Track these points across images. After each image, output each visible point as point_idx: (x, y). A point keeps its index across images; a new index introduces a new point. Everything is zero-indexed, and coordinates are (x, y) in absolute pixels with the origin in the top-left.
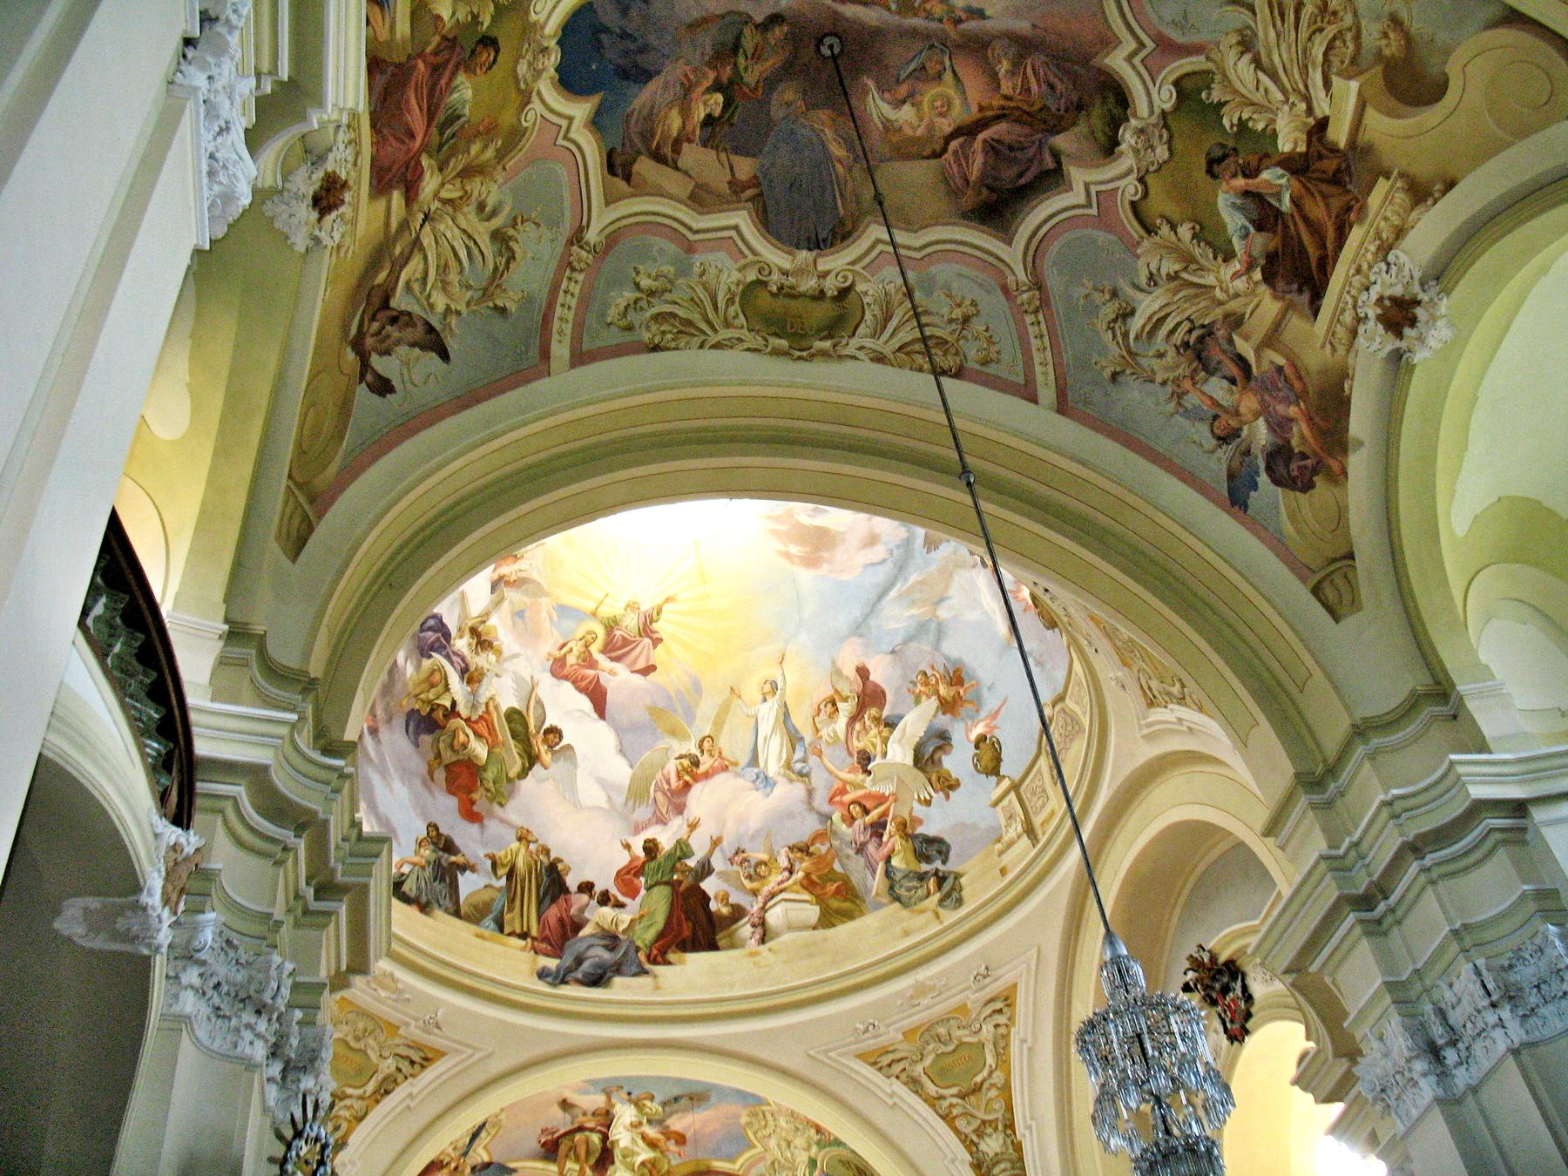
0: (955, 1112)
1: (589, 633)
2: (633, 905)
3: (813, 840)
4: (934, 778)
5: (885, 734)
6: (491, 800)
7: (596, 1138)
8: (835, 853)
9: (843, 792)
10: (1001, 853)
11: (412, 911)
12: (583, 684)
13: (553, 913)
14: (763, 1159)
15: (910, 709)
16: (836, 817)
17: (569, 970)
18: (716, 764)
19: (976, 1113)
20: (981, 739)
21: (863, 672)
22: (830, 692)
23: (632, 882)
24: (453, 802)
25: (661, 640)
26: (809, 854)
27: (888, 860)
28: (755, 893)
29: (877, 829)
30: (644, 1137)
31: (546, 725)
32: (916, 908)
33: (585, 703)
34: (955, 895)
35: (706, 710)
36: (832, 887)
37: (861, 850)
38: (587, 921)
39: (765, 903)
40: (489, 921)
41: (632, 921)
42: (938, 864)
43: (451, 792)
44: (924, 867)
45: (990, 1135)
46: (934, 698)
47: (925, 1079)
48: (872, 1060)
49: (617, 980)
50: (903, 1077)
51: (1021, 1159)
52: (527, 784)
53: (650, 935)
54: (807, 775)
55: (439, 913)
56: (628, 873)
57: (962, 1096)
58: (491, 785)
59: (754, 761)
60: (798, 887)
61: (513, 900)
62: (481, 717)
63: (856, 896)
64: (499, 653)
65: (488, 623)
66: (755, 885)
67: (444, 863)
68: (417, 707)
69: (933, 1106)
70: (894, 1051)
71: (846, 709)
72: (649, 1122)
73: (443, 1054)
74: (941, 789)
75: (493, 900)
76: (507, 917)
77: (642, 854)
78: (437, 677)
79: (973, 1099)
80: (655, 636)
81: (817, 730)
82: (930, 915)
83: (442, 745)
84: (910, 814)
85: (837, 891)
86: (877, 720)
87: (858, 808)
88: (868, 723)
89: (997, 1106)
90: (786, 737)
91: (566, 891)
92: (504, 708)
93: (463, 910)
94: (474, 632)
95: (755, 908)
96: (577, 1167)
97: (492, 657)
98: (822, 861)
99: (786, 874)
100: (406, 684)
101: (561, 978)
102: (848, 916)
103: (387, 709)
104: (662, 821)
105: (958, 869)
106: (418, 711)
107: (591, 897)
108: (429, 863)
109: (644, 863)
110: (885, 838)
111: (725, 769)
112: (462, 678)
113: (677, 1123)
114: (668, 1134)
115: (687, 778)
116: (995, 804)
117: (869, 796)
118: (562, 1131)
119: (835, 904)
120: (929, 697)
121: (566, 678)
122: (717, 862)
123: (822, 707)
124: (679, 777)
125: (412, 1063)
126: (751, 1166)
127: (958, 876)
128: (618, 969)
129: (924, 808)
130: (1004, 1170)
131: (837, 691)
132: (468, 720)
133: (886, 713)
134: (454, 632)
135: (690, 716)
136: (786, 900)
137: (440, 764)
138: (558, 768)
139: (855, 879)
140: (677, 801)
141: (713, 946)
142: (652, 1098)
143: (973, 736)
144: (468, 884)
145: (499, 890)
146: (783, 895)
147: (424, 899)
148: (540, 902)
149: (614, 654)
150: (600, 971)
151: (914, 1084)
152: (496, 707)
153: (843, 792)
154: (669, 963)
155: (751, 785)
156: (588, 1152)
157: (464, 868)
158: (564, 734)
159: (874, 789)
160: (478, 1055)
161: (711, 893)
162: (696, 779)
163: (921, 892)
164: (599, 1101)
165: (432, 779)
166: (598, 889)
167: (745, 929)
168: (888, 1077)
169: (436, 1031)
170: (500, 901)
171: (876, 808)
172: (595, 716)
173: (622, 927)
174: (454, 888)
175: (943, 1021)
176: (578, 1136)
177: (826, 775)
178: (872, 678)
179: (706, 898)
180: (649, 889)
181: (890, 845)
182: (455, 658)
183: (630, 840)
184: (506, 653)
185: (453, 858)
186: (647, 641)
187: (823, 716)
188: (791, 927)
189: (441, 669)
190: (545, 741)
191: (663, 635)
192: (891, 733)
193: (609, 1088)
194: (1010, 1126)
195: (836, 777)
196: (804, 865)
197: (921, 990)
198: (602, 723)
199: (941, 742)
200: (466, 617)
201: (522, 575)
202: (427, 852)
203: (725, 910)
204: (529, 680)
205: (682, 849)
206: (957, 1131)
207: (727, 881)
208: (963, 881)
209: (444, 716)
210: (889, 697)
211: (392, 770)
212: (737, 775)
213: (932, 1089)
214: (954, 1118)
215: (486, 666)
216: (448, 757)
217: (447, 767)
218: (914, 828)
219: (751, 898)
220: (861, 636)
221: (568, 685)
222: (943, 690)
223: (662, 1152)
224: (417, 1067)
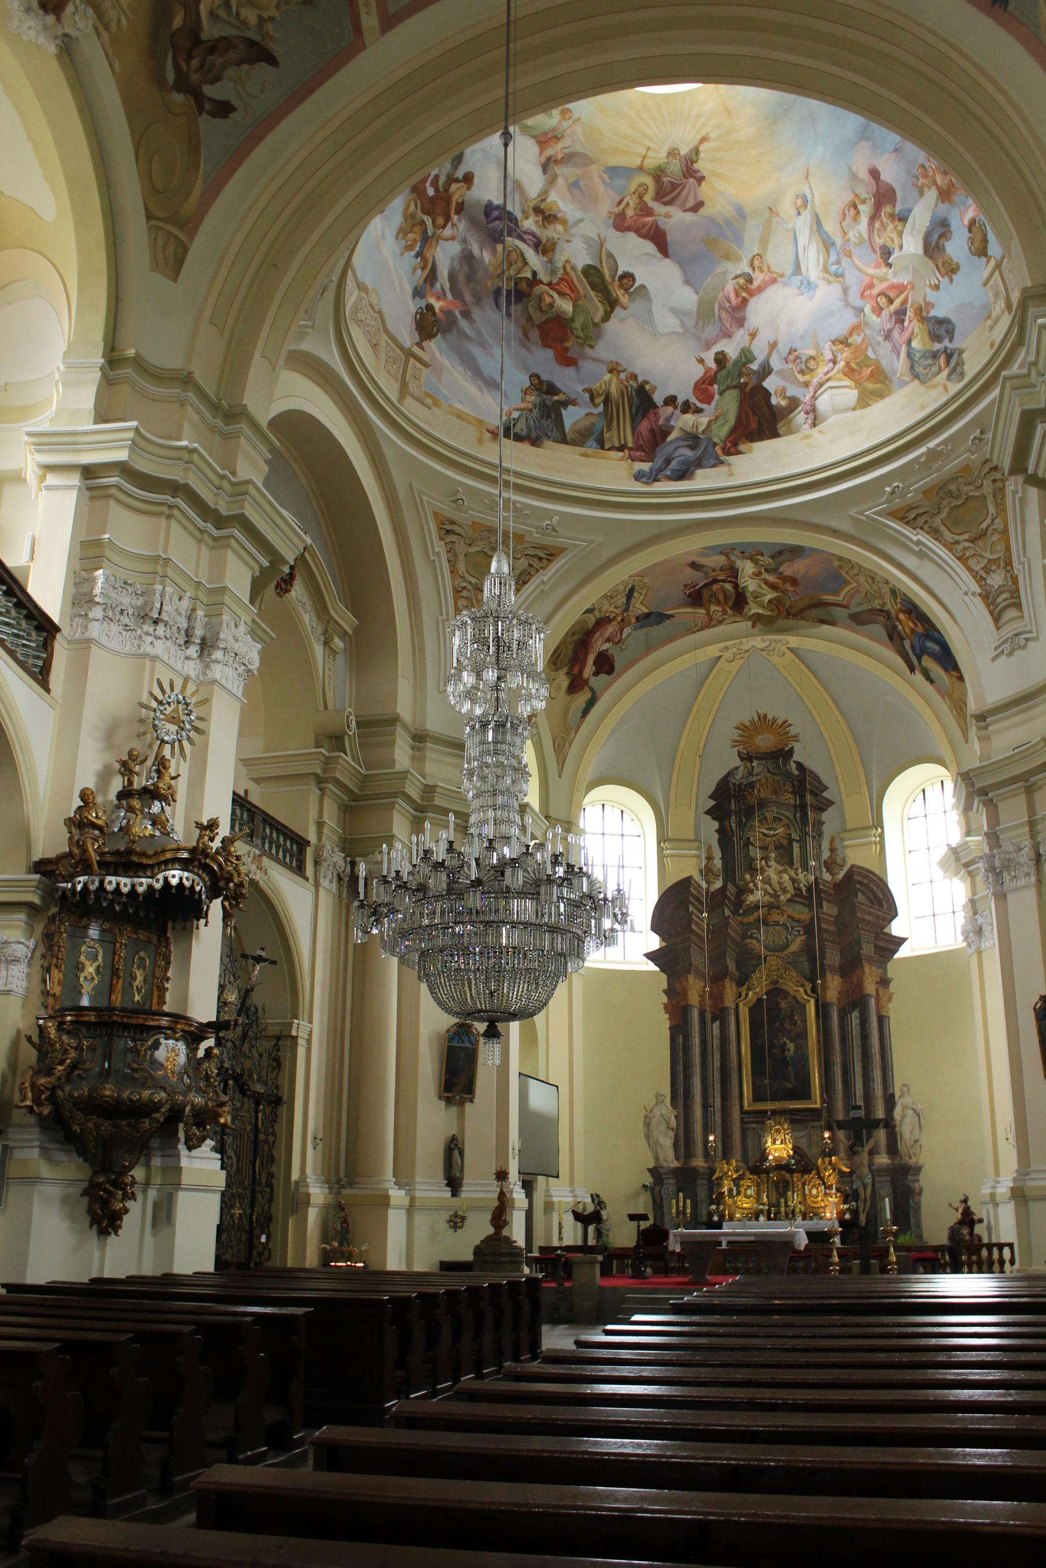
0: (968, 554)
1: (640, 185)
2: (709, 409)
3: (851, 333)
4: (940, 264)
5: (899, 228)
6: (582, 345)
7: (729, 587)
8: (867, 343)
9: (871, 286)
10: (991, 328)
11: (526, 447)
12: (645, 231)
13: (644, 426)
14: (858, 591)
15: (917, 201)
16: (868, 309)
17: (660, 470)
18: (767, 278)
19: (983, 553)
20: (973, 222)
21: (875, 174)
22: (851, 197)
23: (707, 389)
24: (550, 353)
25: (702, 179)
26: (848, 345)
27: (909, 342)
28: (806, 385)
29: (900, 316)
30: (766, 582)
31: (620, 272)
32: (930, 383)
33: (649, 247)
34: (959, 369)
35: (752, 232)
36: (867, 372)
37: (888, 336)
38: (673, 428)
39: (815, 393)
40: (591, 442)
41: (710, 422)
42: (946, 343)
43: (546, 345)
44: (937, 346)
45: (994, 571)
46: (933, 188)
47: (943, 528)
48: (901, 516)
49: (699, 472)
50: (926, 527)
51: (1018, 590)
52: (611, 325)
53: (724, 431)
54: (842, 276)
55: (548, 443)
56: (703, 383)
57: (973, 540)
58: (581, 334)
59: (797, 269)
60: (840, 375)
61: (609, 422)
62: (561, 279)
63: (886, 378)
64: (564, 222)
65: (549, 200)
66: (806, 378)
67: (548, 402)
69: (950, 550)
70: (917, 507)
71: (865, 210)
72: (767, 571)
73: (562, 550)
74: (947, 274)
75: (593, 424)
76: (607, 435)
77: (713, 365)
78: (514, 256)
79: (980, 543)
80: (698, 175)
81: (845, 234)
82: (940, 388)
83: (531, 310)
84: (924, 299)
85: (872, 375)
86: (892, 216)
87: (884, 299)
88: (885, 220)
89: (999, 547)
90: (821, 247)
91: (653, 405)
92: (580, 268)
93: (568, 438)
94: (537, 210)
95: (808, 398)
96: (720, 609)
97: (560, 228)
98: (859, 351)
99: (831, 365)
100: (486, 270)
101: (653, 477)
102: (880, 395)
103: (474, 293)
104: (728, 335)
105: (961, 346)
107: (675, 407)
108: (535, 406)
109: (716, 373)
110: (906, 324)
111: (774, 281)
112: (536, 250)
113: (787, 569)
114: (784, 579)
115: (744, 294)
116: (986, 284)
117: (893, 287)
118: (701, 585)
119: (870, 386)
120: (930, 188)
121: (628, 229)
122: (775, 363)
123: (846, 211)
124: (737, 295)
125: (541, 559)
126: (852, 597)
127: (961, 352)
128: (699, 464)
129: (934, 293)
130: (1005, 600)
131: (856, 195)
132: (549, 285)
133: (897, 209)
134: (518, 214)
135: (739, 238)
136: (831, 388)
137: (532, 325)
138: (636, 307)
139: (885, 364)
140: (739, 315)
141: (775, 434)
142: (762, 555)
143: (966, 223)
144: (571, 417)
145: (598, 415)
146: (829, 384)
147: (534, 435)
148: (633, 420)
149: (667, 199)
150: (685, 467)
151: (935, 533)
152: (573, 268)
153: (871, 286)
154: (740, 453)
155: (797, 291)
156: (726, 598)
157: (565, 404)
158: (637, 276)
159: (895, 281)
160: (592, 546)
161: (772, 390)
162: (751, 294)
163: (934, 369)
164: (722, 560)
165: (528, 339)
166: (680, 401)
167: (800, 417)
168: (914, 529)
169: (554, 533)
170: (601, 423)
171: (898, 296)
172: (660, 256)
173: (701, 429)
174: (559, 421)
175: (953, 479)
176: (715, 587)
177: (856, 273)
178: (882, 178)
179: (767, 394)
180: (721, 394)
181: (910, 329)
182: (526, 237)
183: (703, 356)
184: (571, 221)
185: (556, 398)
186: (692, 180)
187: (848, 220)
188: (836, 411)
189: (516, 248)
190: (621, 286)
191: (705, 174)
192: (904, 226)
193: (726, 550)
194: (1009, 563)
195: (865, 273)
196: (844, 355)
197: (932, 454)
198: (667, 261)
199: (943, 230)
200: (527, 200)
201: (569, 150)
202: (532, 398)
203: (783, 403)
204: (597, 238)
205: (747, 356)
206: (970, 569)
207: (783, 378)
208: (965, 356)
209: (528, 285)
210: (899, 193)
211: (490, 341)
212: (785, 285)
213: (949, 536)
214: (967, 558)
215: (556, 236)
216: (538, 317)
217: (539, 327)
218: (928, 313)
219: (804, 390)
220: (867, 139)
221: (632, 236)
222: (939, 179)
223: (783, 592)
224: (545, 561)
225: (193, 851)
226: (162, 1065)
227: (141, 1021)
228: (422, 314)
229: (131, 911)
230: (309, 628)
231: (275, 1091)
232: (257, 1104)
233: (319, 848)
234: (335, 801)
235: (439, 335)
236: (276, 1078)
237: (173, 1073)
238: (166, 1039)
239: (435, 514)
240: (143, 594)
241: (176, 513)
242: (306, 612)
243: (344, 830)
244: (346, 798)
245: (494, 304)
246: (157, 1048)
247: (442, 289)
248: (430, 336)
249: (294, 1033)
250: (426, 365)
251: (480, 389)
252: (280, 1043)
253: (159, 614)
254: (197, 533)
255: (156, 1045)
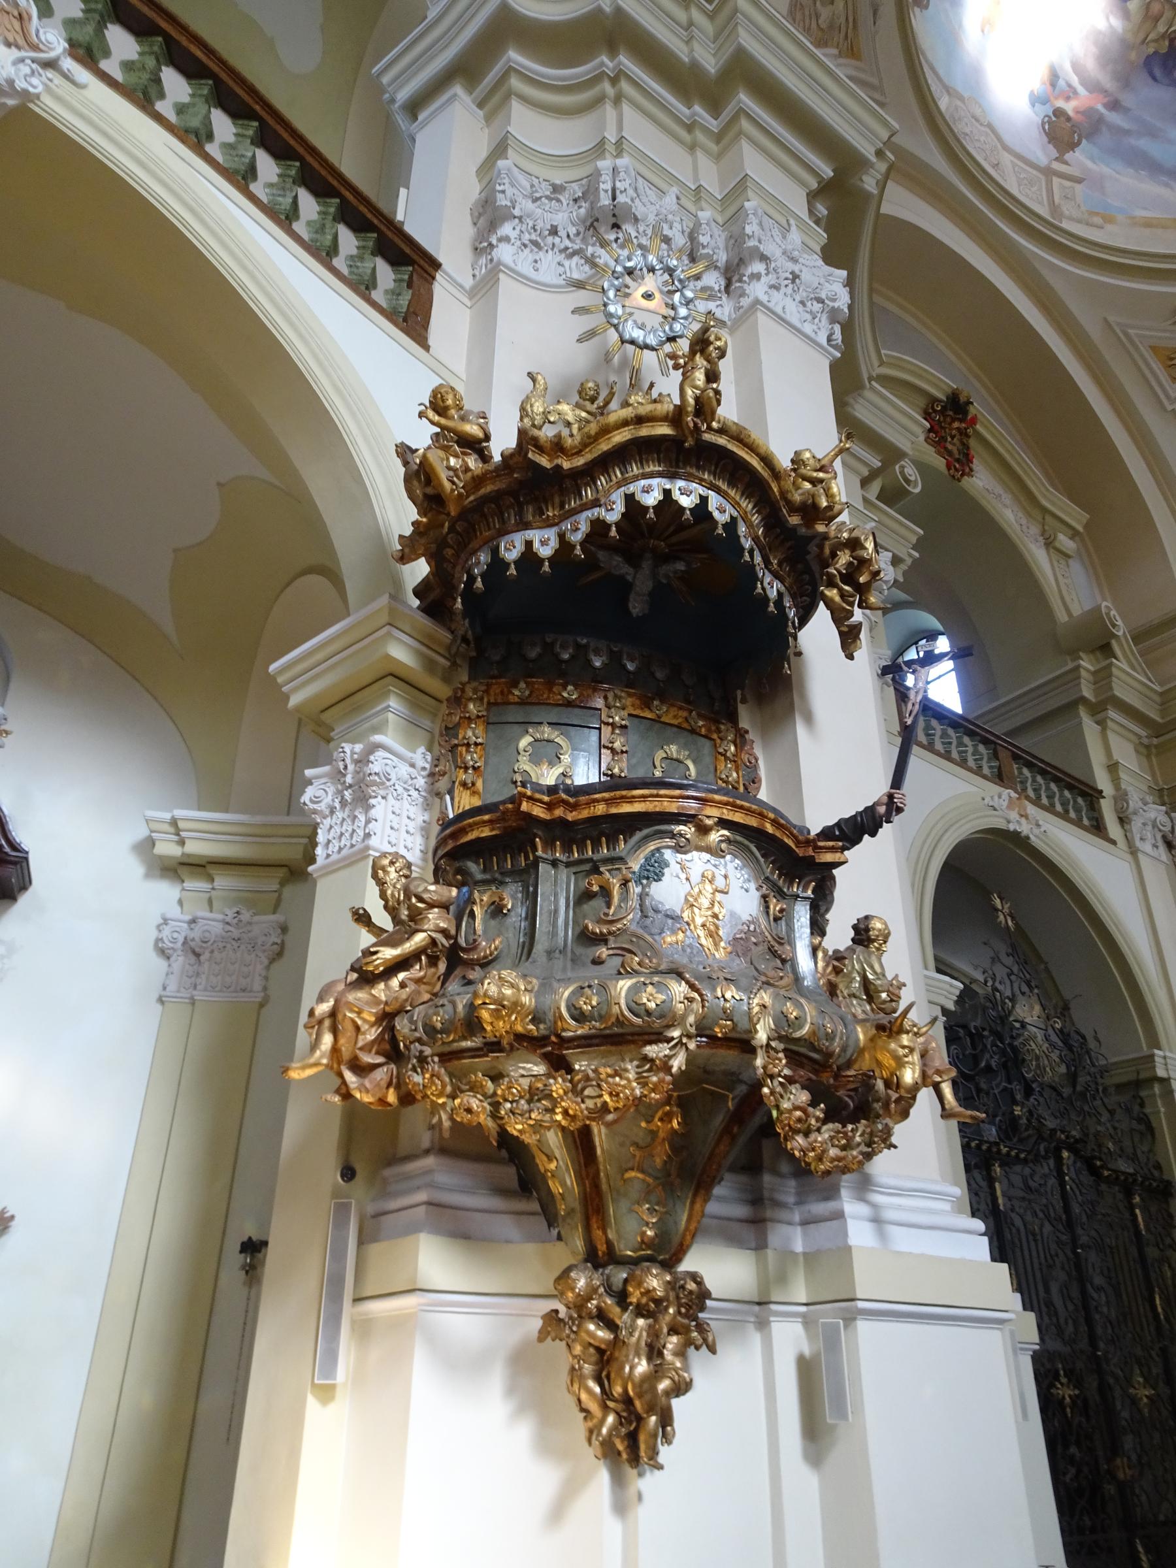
68: (1151, 50)
106: (1156, 53)
225: (676, 417)
226: (675, 918)
227: (600, 809)
228: (1049, 122)
229: (630, 667)
230: (1018, 528)
231: (1156, 1173)
232: (1129, 1194)
233: (1121, 798)
234: (1129, 740)
235: (1084, 141)
236: (1150, 1151)
237: (713, 935)
238: (679, 849)
239: (1154, 349)
240: (585, 196)
241: (625, 86)
242: (1005, 506)
243: (1153, 775)
244: (1143, 733)
245: (1150, 80)
246: (658, 877)
247: (1070, 86)
248: (1073, 146)
249: (1161, 1073)
250: (1079, 181)
251: (1167, 185)
252: (1143, 1094)
253: (614, 199)
254: (683, 134)
255: (654, 871)
